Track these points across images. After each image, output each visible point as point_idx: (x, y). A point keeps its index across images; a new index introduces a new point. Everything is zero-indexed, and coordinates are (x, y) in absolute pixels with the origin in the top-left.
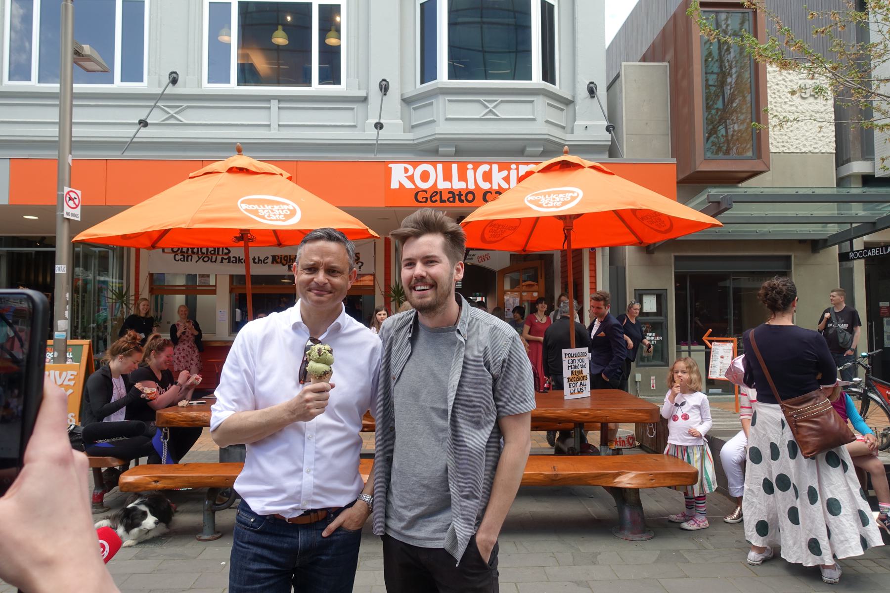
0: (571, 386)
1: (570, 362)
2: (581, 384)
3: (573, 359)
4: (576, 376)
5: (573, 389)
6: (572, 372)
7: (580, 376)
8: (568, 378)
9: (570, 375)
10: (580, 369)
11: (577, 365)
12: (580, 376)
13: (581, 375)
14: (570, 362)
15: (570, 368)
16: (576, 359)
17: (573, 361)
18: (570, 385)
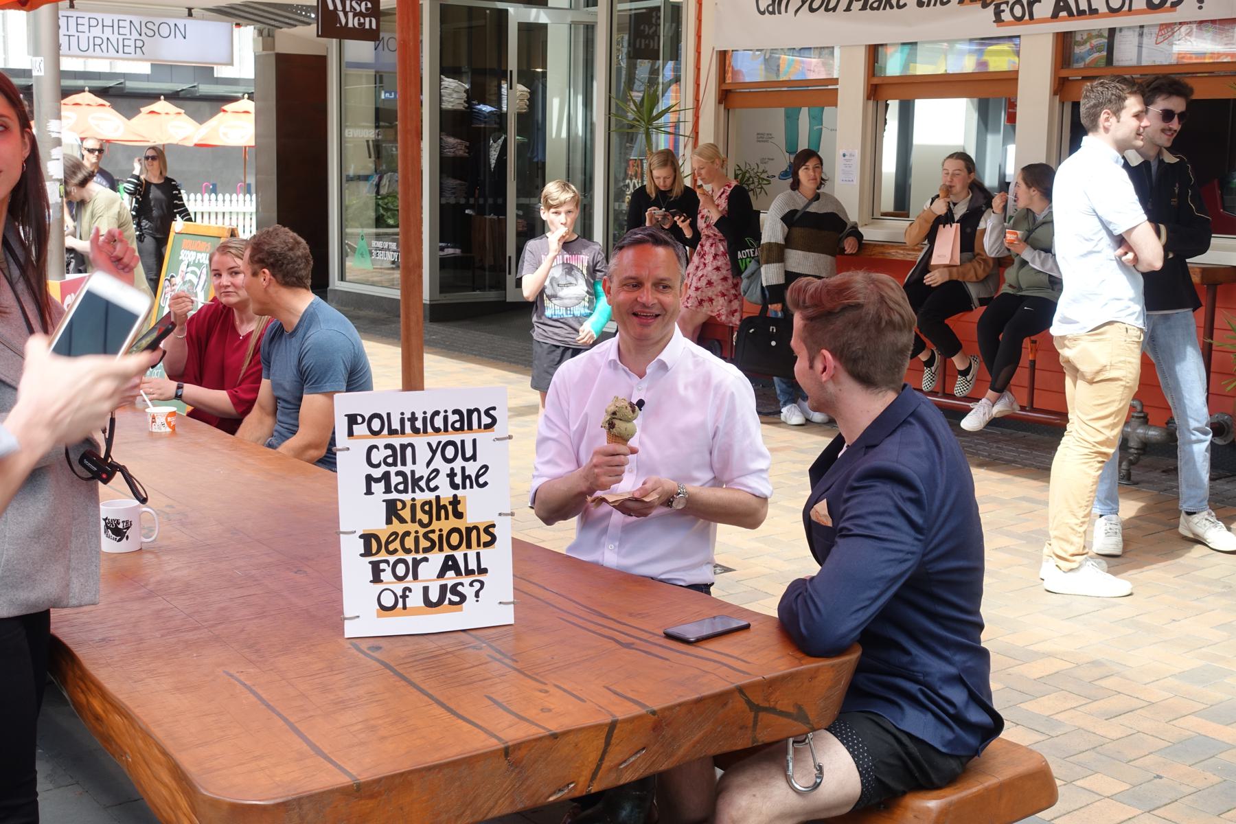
0: (387, 576)
1: (377, 457)
2: (450, 565)
3: (397, 441)
4: (412, 527)
5: (398, 588)
6: (392, 510)
7: (445, 525)
8: (367, 538)
9: (376, 521)
10: (446, 493)
11: (422, 471)
12: (445, 525)
13: (453, 522)
14: (377, 457)
15: (378, 488)
16: (420, 442)
17: (398, 455)
18: (376, 567)
